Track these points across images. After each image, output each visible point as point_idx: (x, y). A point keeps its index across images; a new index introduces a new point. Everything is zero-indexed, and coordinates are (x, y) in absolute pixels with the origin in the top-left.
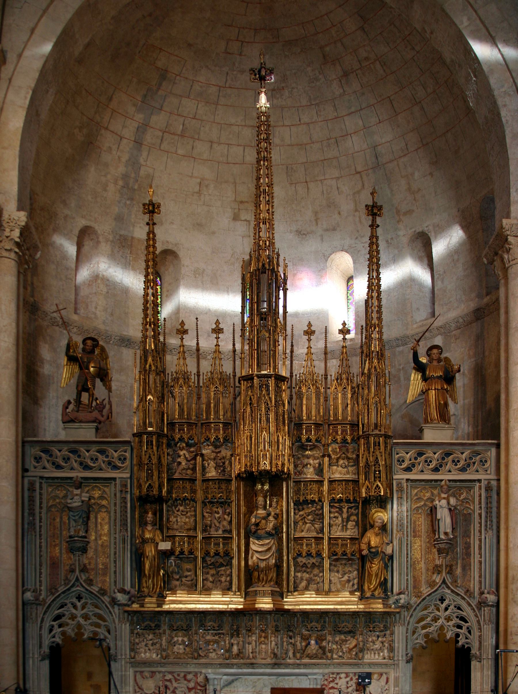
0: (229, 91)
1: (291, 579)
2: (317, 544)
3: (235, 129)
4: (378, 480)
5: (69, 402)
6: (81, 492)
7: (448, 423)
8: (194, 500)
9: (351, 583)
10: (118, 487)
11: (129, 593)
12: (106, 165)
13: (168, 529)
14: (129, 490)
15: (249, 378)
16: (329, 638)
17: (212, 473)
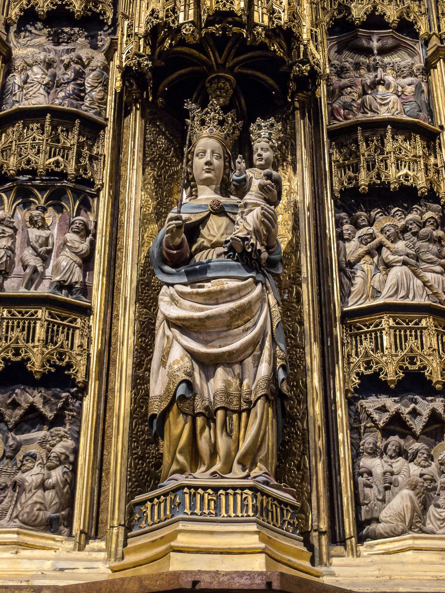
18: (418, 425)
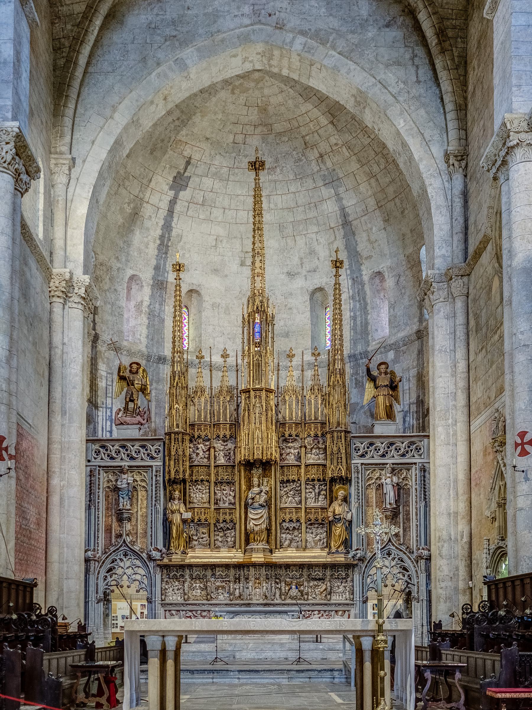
0: (236, 171)
1: (278, 538)
2: (296, 513)
3: (242, 198)
4: (340, 464)
5: (120, 410)
6: (128, 477)
7: (393, 421)
8: (208, 481)
9: (322, 542)
10: (154, 473)
11: (161, 551)
12: (148, 229)
13: (190, 502)
14: (162, 474)
15: (247, 391)
16: (306, 584)
17: (222, 461)
18: (291, 529)
